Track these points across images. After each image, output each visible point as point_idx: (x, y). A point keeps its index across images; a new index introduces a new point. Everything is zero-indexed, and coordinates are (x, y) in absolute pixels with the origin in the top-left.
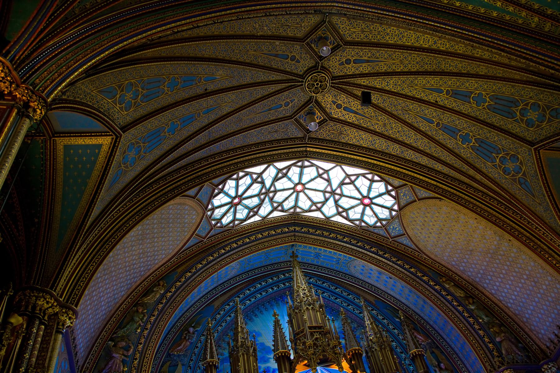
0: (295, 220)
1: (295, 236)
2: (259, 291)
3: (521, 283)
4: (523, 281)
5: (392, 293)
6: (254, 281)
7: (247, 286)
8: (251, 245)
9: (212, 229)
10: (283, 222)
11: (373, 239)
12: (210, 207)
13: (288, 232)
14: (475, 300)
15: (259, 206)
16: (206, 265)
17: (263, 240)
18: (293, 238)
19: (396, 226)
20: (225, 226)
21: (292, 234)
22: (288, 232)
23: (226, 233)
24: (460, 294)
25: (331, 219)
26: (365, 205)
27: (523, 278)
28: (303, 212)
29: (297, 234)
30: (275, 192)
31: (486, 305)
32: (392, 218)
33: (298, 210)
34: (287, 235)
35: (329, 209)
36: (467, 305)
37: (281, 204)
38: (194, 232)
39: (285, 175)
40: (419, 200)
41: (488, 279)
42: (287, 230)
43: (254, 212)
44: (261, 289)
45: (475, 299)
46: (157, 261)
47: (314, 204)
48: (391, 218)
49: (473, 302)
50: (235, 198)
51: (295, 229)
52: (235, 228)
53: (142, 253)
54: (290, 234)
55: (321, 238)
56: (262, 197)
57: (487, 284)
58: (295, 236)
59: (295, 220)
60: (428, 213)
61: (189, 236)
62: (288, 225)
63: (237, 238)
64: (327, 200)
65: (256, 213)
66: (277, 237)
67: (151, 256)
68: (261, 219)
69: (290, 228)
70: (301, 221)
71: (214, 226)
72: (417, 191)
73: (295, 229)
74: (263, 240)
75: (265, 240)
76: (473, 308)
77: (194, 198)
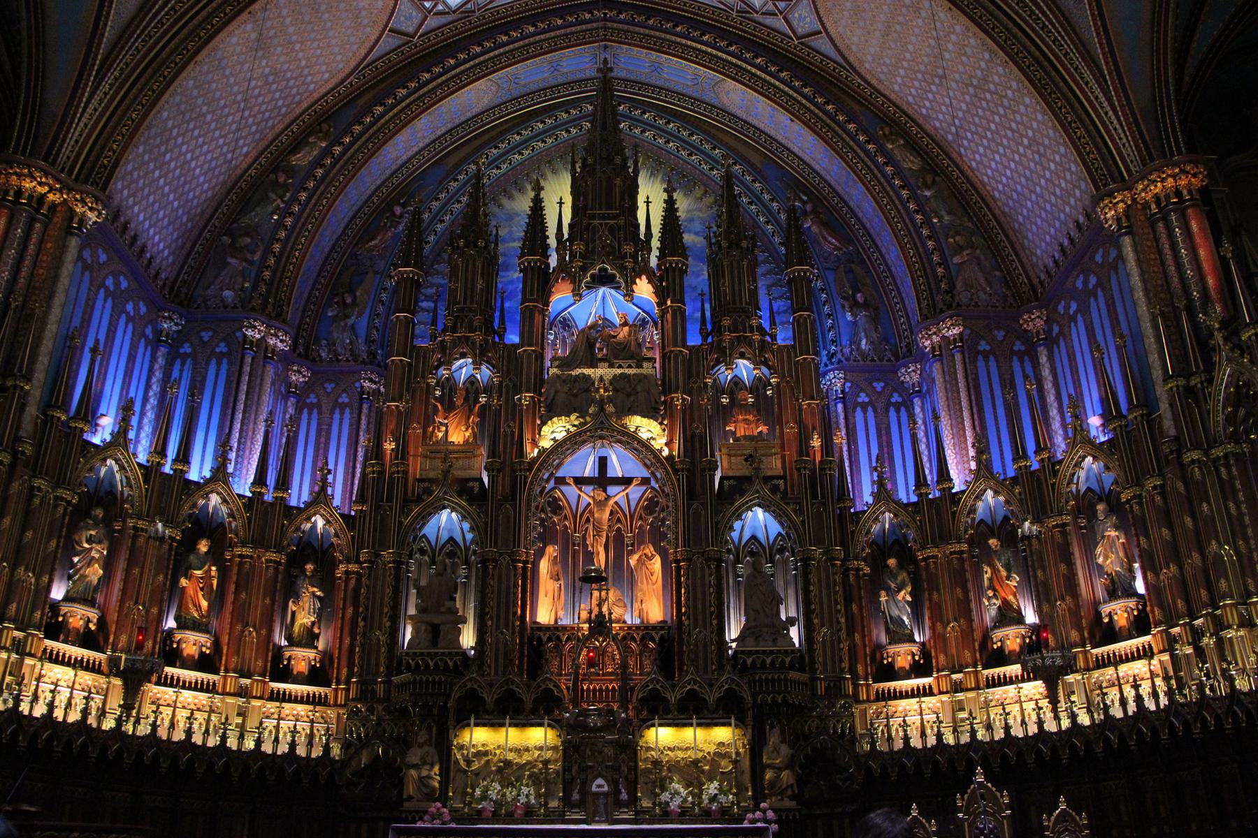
1: (605, 28)
2: (541, 136)
7: (514, 126)
8: (511, 47)
9: (426, 17)
11: (760, 38)
13: (590, 21)
16: (417, 90)
17: (537, 38)
20: (454, 12)
22: (590, 21)
24: (911, 163)
29: (609, 24)
31: (957, 189)
36: (919, 188)
38: (386, 26)
44: (545, 132)
46: (312, 86)
49: (934, 182)
51: (605, 14)
53: (270, 74)
54: (595, 25)
55: (658, 34)
58: (605, 28)
61: (377, 34)
66: (568, 30)
67: (296, 78)
71: (430, 12)
73: (605, 14)
74: (537, 38)
75: (542, 37)
76: (927, 193)
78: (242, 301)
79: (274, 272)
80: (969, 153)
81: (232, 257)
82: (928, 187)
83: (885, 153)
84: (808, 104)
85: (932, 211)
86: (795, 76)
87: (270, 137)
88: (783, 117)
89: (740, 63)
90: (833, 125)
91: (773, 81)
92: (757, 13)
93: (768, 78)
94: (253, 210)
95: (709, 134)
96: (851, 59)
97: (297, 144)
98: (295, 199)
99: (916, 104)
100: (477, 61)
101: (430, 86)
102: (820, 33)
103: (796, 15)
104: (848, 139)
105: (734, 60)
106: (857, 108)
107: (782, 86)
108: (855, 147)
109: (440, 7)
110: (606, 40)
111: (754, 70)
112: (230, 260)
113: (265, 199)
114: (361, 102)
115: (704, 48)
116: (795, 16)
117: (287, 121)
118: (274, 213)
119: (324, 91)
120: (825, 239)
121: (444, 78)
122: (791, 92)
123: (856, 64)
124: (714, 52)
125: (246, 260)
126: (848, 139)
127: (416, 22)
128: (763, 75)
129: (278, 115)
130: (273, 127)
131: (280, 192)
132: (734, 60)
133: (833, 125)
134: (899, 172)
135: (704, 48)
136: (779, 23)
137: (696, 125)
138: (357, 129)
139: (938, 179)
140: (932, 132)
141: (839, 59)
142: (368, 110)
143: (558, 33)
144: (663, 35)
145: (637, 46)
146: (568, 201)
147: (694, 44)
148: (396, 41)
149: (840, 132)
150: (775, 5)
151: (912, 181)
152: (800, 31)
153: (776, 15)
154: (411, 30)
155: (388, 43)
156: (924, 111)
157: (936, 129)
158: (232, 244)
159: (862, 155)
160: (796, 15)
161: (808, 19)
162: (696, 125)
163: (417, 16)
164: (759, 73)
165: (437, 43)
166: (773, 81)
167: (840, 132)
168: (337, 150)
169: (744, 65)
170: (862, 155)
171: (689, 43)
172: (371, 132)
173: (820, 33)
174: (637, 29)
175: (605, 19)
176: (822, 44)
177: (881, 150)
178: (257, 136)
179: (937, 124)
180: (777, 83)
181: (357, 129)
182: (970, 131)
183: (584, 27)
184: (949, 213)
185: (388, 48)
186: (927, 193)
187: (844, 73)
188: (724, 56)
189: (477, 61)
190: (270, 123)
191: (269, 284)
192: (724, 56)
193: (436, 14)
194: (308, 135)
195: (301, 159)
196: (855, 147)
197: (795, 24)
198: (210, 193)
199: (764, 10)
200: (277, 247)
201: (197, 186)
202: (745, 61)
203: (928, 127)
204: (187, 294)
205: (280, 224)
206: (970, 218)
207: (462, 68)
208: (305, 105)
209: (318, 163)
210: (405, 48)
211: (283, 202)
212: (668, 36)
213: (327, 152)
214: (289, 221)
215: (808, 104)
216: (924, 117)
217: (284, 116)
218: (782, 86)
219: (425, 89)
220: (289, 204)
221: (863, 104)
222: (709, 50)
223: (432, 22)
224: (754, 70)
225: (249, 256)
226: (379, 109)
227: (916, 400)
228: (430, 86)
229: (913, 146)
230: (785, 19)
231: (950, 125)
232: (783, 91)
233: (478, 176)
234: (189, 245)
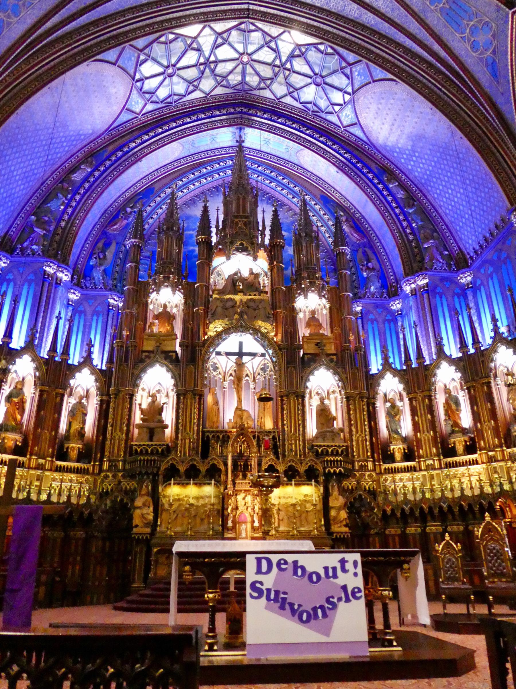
1: (241, 118)
6: (200, 165)
9: (146, 104)
12: (138, 77)
14: (415, 203)
15: (199, 79)
18: (240, 120)
19: (348, 113)
23: (164, 109)
24: (401, 195)
25: (282, 100)
26: (318, 85)
29: (244, 116)
30: (217, 62)
32: (345, 103)
33: (247, 87)
34: (233, 116)
35: (279, 89)
37: (225, 77)
39: (226, 41)
40: (374, 81)
41: (433, 182)
42: (233, 110)
43: (193, 86)
44: (207, 174)
45: (415, 201)
47: (263, 79)
48: (342, 102)
50: (168, 67)
51: (242, 110)
52: (174, 104)
54: (236, 116)
56: (202, 67)
57: (432, 187)
58: (241, 118)
59: (242, 99)
60: (383, 98)
62: (234, 106)
64: (276, 75)
65: (196, 88)
68: (204, 95)
69: (237, 109)
71: (148, 101)
72: (372, 70)
73: (242, 110)
76: (411, 211)
77: (114, 64)
78: (43, 251)
79: (61, 237)
80: (433, 189)
81: (38, 228)
82: (410, 207)
84: (347, 163)
85: (413, 219)
87: (59, 163)
88: (333, 170)
89: (312, 140)
91: (329, 150)
92: (323, 112)
94: (49, 203)
95: (292, 179)
96: (371, 139)
97: (73, 170)
98: (72, 198)
99: (405, 163)
100: (173, 131)
101: (148, 143)
102: (356, 124)
103: (344, 114)
105: (309, 138)
107: (334, 153)
109: (154, 99)
110: (241, 124)
111: (319, 144)
112: (36, 229)
113: (57, 197)
115: (293, 131)
116: (343, 115)
117: (69, 155)
118: (61, 205)
119: (89, 141)
120: (352, 235)
121: (155, 139)
122: (338, 156)
123: (374, 142)
124: (299, 133)
125: (44, 229)
127: (141, 106)
129: (64, 151)
130: (60, 158)
132: (309, 138)
134: (395, 199)
136: (333, 118)
137: (285, 175)
139: (415, 203)
141: (365, 139)
142: (114, 153)
143: (216, 119)
144: (272, 123)
145: (258, 128)
146: (221, 208)
148: (130, 116)
150: (333, 108)
151: (402, 205)
152: (345, 123)
153: (332, 113)
154: (138, 110)
155: (125, 117)
156: (410, 167)
157: (416, 177)
158: (37, 220)
160: (344, 114)
161: (350, 117)
162: (285, 175)
163: (141, 103)
164: (322, 145)
166: (329, 150)
168: (97, 174)
169: (314, 141)
171: (286, 128)
172: (115, 165)
173: (356, 124)
174: (258, 119)
175: (241, 112)
176: (356, 131)
177: (387, 188)
178: (52, 162)
179: (416, 174)
180: (331, 151)
182: (435, 177)
183: (230, 116)
184: (422, 221)
185: (125, 120)
186: (411, 211)
188: (304, 136)
189: (173, 131)
190: (59, 155)
191: (59, 244)
192: (304, 136)
193: (151, 102)
194: (81, 164)
195: (77, 177)
197: (342, 119)
198: (24, 191)
199: (327, 111)
200: (63, 224)
201: (17, 186)
203: (411, 177)
204: (10, 247)
205: (64, 211)
206: (432, 224)
207: (165, 134)
208: (79, 147)
209: (86, 179)
210: (135, 121)
211: (66, 199)
212: (275, 124)
213: (91, 174)
214: (70, 210)
217: (67, 152)
219: (145, 144)
220: (70, 200)
221: (376, 163)
222: (296, 132)
223: (150, 107)
224: (319, 144)
225: (47, 228)
226: (120, 154)
228: (148, 143)
229: (402, 186)
230: (338, 116)
231: (424, 175)
232: (334, 156)
233: (173, 194)
234: (12, 220)
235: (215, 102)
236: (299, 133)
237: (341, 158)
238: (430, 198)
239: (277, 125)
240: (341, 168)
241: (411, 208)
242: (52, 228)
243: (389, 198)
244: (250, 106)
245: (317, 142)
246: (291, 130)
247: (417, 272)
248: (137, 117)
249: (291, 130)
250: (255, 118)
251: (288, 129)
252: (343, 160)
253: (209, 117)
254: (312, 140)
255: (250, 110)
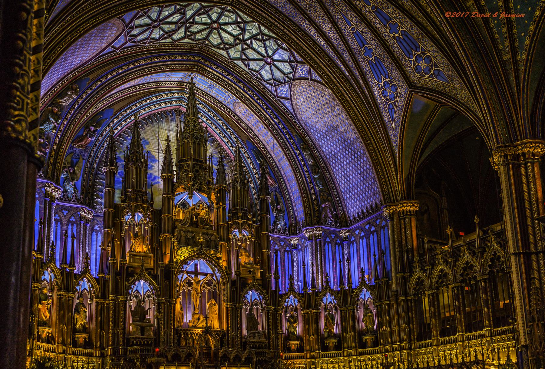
0: (201, 51)
1: (198, 66)
3: (355, 174)
4: (356, 173)
5: (261, 139)
10: (191, 50)
13: (193, 61)
18: (196, 67)
21: (196, 63)
22: (193, 61)
27: (358, 172)
28: (211, 46)
29: (200, 65)
34: (191, 63)
42: (192, 58)
54: (194, 63)
58: (198, 66)
59: (201, 51)
62: (194, 54)
63: (147, 56)
69: (196, 58)
70: (207, 54)
76: (316, 177)
83: (302, 156)
84: (276, 126)
86: (273, 113)
90: (284, 137)
91: (263, 111)
93: (262, 110)
104: (288, 145)
105: (249, 98)
106: (295, 134)
107: (266, 115)
108: (291, 149)
111: (256, 104)
114: (91, 77)
115: (238, 88)
122: (270, 118)
124: (242, 91)
126: (288, 145)
128: (260, 108)
131: (56, 118)
132: (249, 98)
133: (284, 137)
135: (238, 88)
138: (89, 91)
140: (321, 152)
142: (94, 83)
147: (234, 85)
149: (286, 141)
159: (293, 153)
165: (126, 55)
166: (263, 111)
167: (286, 141)
170: (293, 153)
175: (198, 62)
180: (265, 113)
181: (89, 91)
186: (316, 177)
187: (292, 118)
188: (246, 95)
196: (291, 149)
202: (254, 99)
215: (276, 126)
216: (320, 145)
218: (266, 115)
226: (99, 83)
227: (295, 251)
229: (312, 155)
232: (266, 117)
235: (179, 49)
236: (242, 91)
237: (271, 120)
238: (330, 169)
239: (226, 80)
240: (271, 128)
241: (317, 175)
242: (47, 151)
243: (302, 163)
244: (207, 59)
245: (255, 103)
246: (236, 87)
247: (315, 224)
248: (115, 51)
249: (236, 87)
250: (209, 69)
251: (234, 85)
252: (272, 122)
253: (173, 61)
254: (251, 99)
255: (206, 61)
